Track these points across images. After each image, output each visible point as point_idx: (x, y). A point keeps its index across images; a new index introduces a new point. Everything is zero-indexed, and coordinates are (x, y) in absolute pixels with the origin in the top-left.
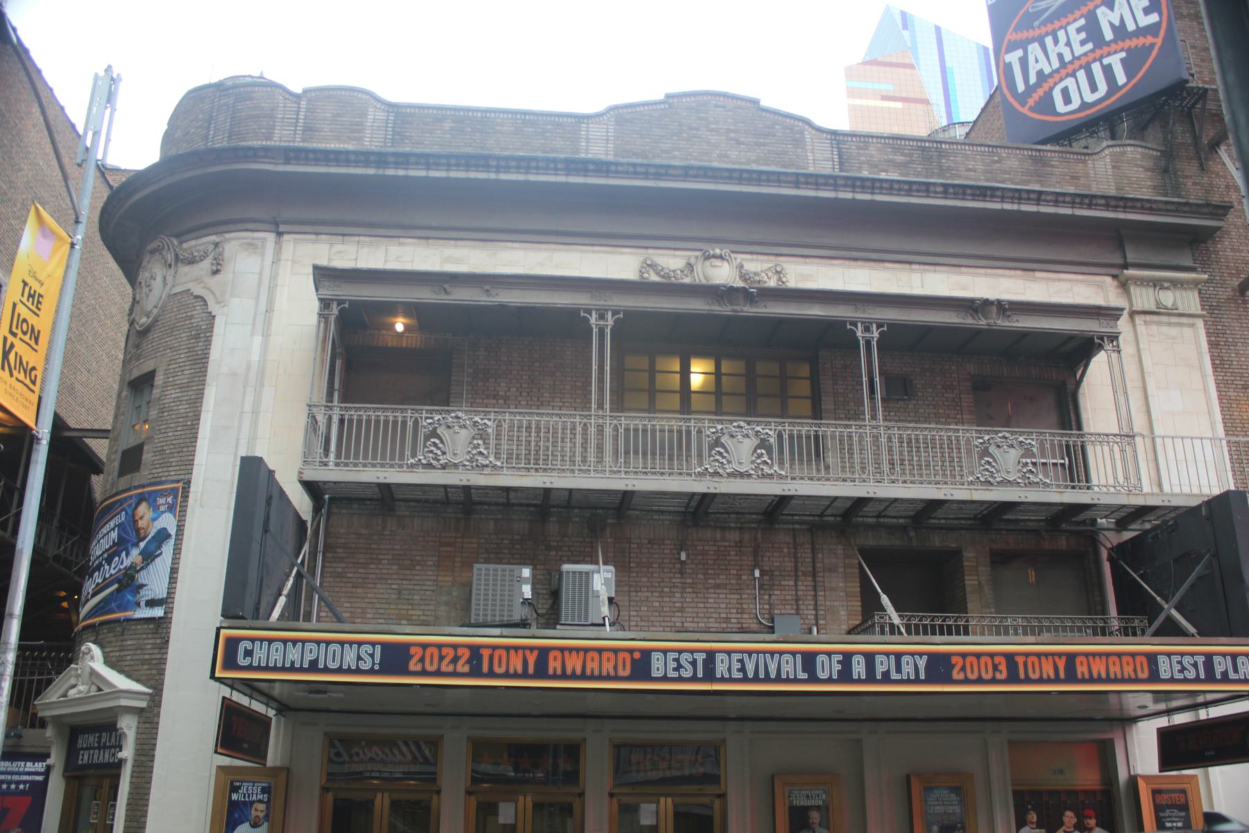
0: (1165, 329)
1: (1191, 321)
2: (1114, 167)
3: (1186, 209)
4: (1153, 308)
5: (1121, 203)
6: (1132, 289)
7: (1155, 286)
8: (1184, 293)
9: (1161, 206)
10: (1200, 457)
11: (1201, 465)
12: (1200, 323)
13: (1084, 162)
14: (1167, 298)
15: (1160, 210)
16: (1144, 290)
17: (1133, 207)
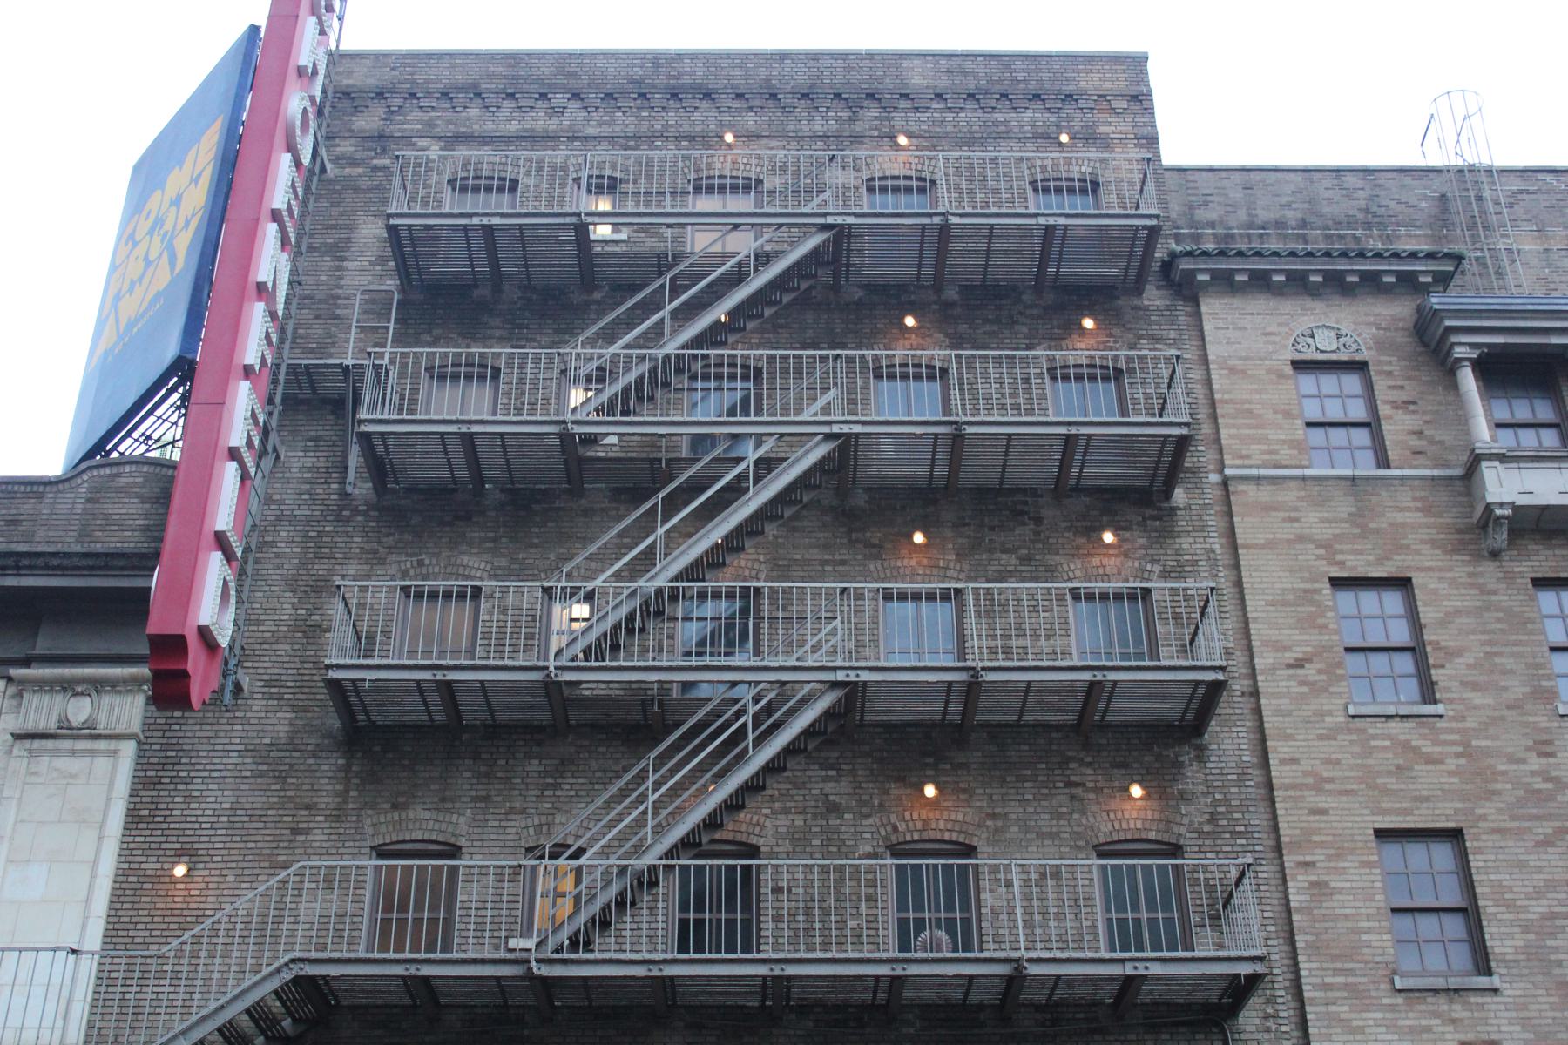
0: (64, 763)
1: (113, 745)
2: (89, 500)
3: (122, 563)
4: (52, 727)
5: (10, 562)
6: (26, 695)
7: (64, 690)
8: (118, 699)
9: (76, 561)
10: (41, 977)
11: (38, 992)
12: (128, 749)
13: (41, 496)
14: (79, 710)
15: (78, 568)
16: (47, 698)
17: (30, 567)
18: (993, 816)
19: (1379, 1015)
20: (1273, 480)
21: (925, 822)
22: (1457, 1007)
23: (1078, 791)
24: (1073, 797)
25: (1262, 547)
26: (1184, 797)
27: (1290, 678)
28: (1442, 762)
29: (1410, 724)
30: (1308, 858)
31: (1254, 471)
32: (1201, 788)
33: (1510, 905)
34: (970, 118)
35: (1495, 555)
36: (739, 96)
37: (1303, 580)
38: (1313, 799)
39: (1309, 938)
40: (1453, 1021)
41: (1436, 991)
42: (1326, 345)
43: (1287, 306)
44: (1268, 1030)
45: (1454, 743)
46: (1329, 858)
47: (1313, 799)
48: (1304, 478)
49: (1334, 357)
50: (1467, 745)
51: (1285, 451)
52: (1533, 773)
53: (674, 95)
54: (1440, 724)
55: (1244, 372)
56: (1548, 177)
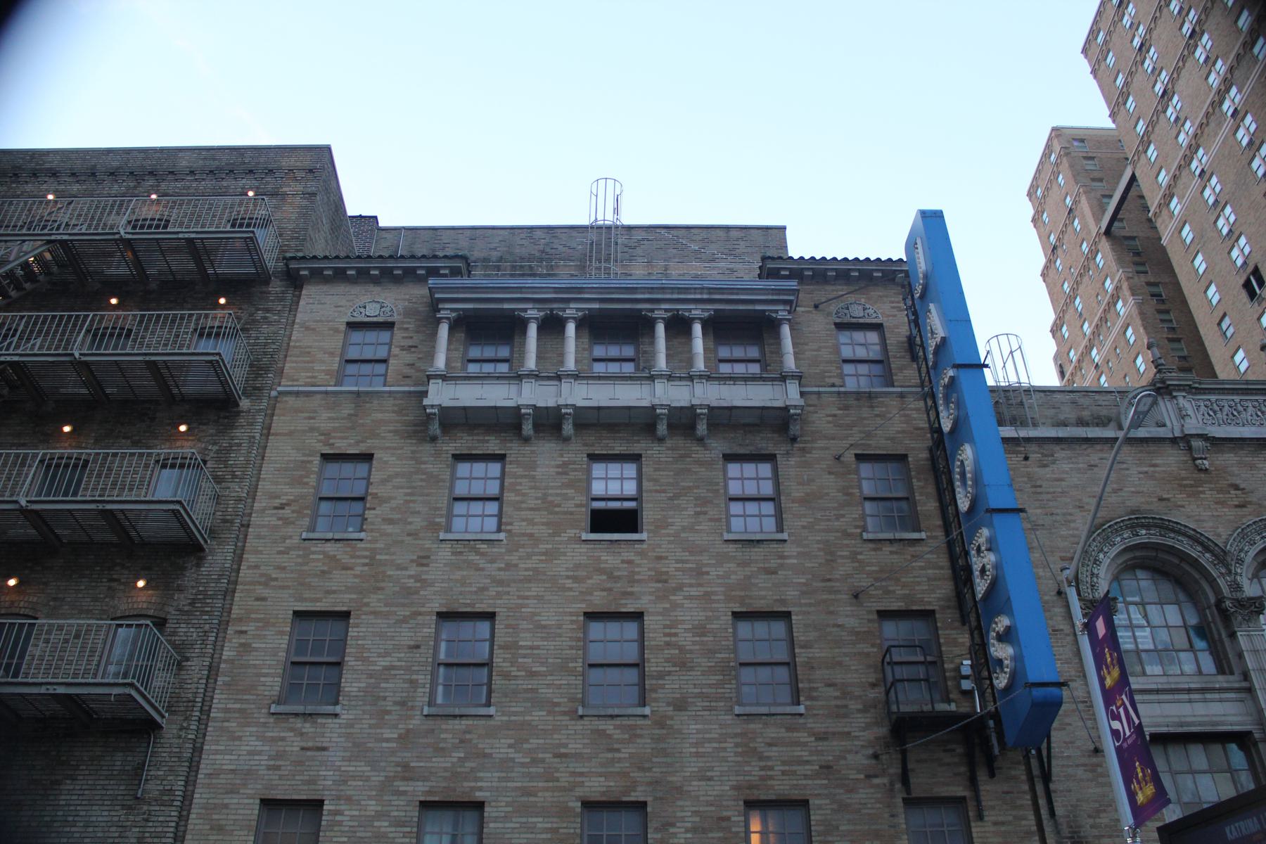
18: (55, 599)
19: (254, 729)
20: (308, 394)
21: (12, 602)
22: (307, 725)
23: (114, 584)
24: (110, 588)
25: (285, 435)
26: (180, 589)
27: (272, 515)
28: (351, 569)
29: (339, 545)
30: (244, 628)
31: (296, 389)
32: (193, 584)
33: (365, 660)
34: (208, 184)
35: (434, 439)
36: (73, 174)
37: (304, 455)
38: (260, 591)
39: (227, 679)
40: (302, 734)
41: (297, 715)
42: (372, 312)
43: (356, 289)
44: (180, 737)
45: (366, 557)
46: (258, 628)
47: (260, 591)
48: (326, 393)
49: (375, 319)
50: (372, 558)
51: (323, 376)
52: (410, 577)
53: (35, 175)
54: (360, 545)
55: (314, 329)
56: (663, 231)
